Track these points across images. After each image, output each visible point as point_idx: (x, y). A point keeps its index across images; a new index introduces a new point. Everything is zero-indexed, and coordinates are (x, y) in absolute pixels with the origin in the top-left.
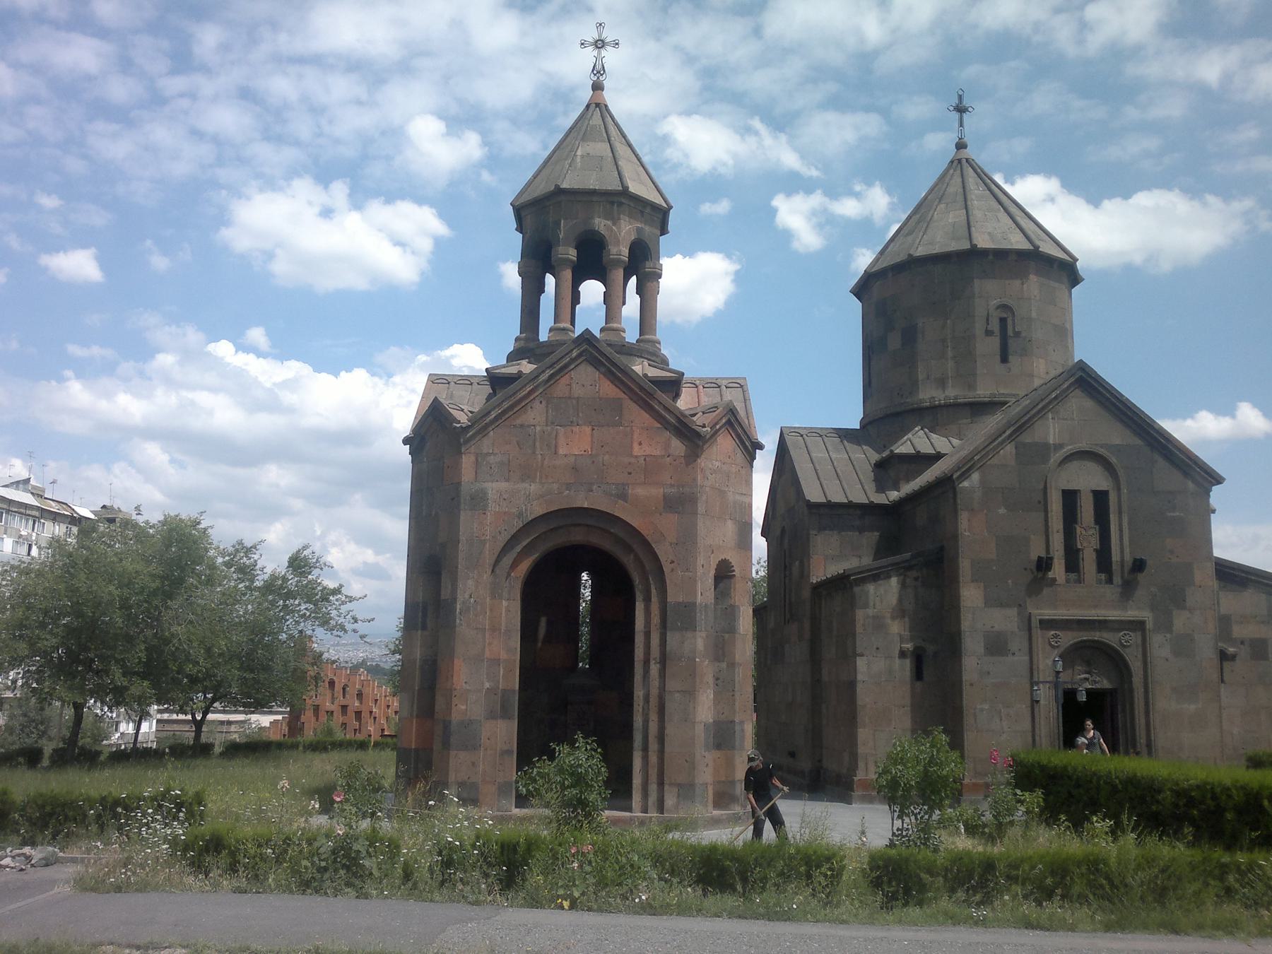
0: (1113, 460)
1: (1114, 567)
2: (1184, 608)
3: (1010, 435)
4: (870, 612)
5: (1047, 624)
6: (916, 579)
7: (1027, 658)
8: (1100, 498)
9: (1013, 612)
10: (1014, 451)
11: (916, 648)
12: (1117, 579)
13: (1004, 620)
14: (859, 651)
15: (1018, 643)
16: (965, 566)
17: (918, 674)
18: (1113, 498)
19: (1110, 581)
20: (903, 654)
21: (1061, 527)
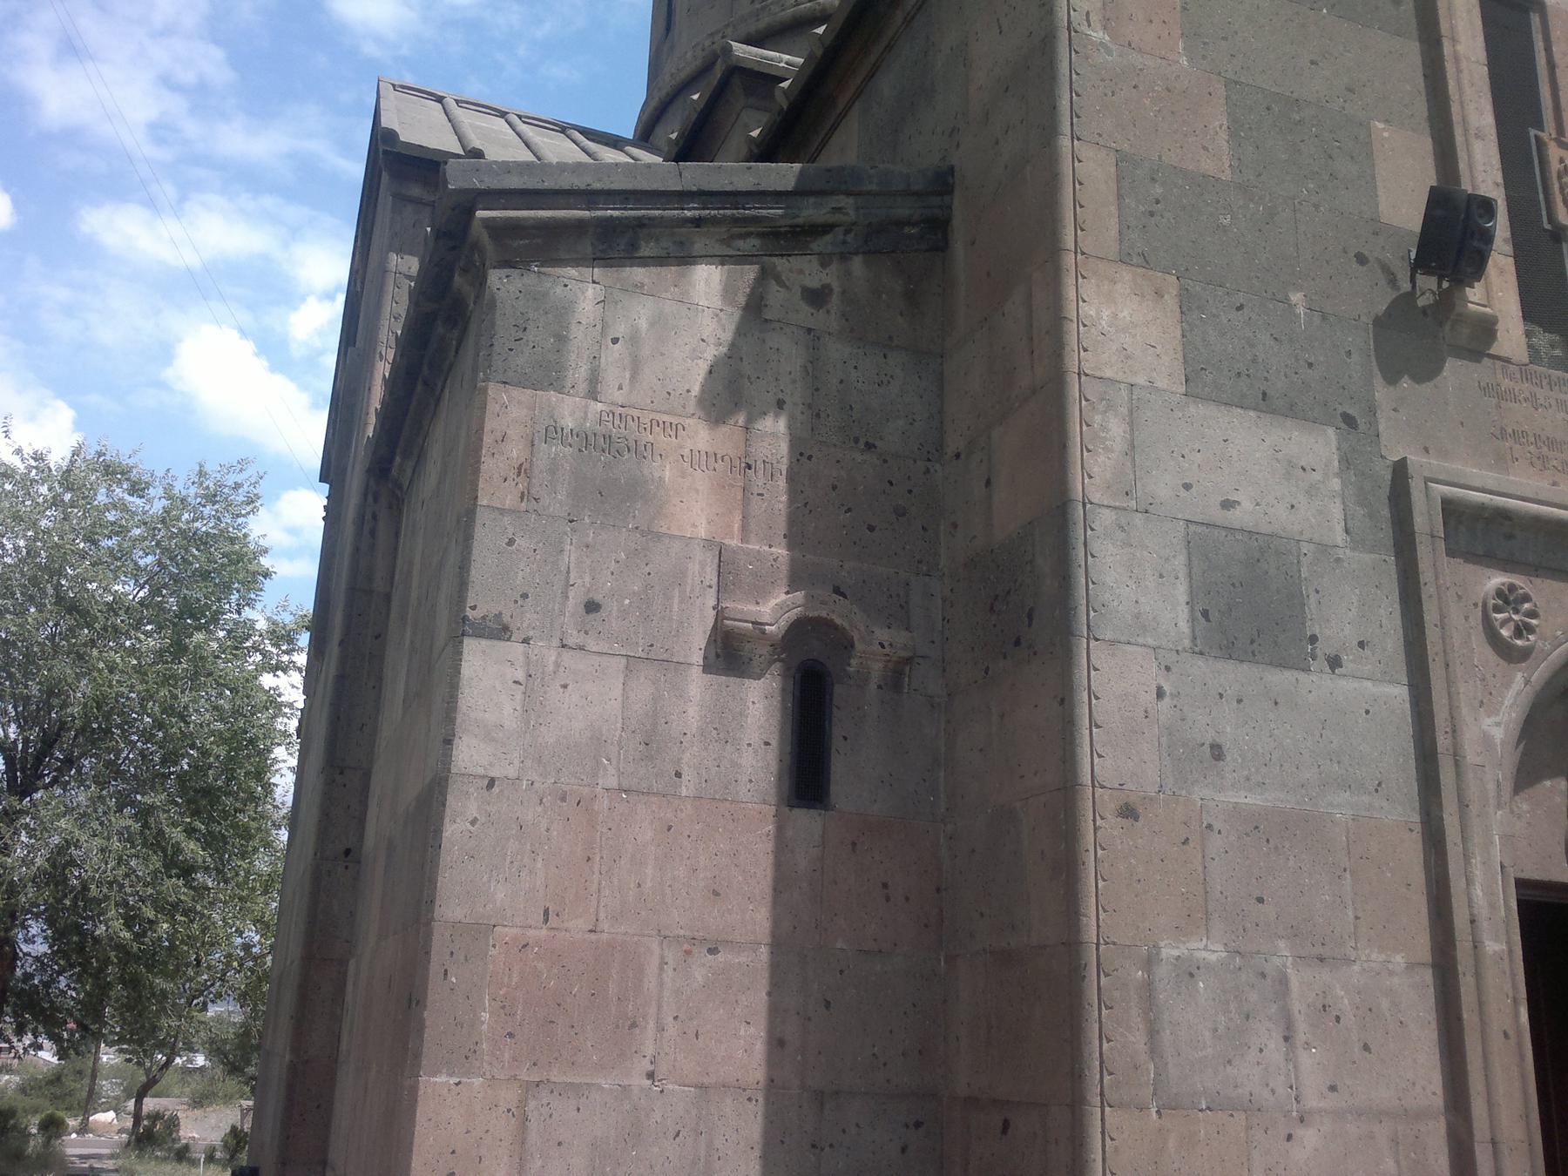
4: (570, 410)
5: (1483, 532)
6: (817, 297)
7: (1398, 694)
9: (1318, 447)
11: (800, 629)
13: (1279, 478)
14: (481, 603)
15: (1352, 607)
16: (1088, 171)
17: (807, 774)
20: (728, 652)
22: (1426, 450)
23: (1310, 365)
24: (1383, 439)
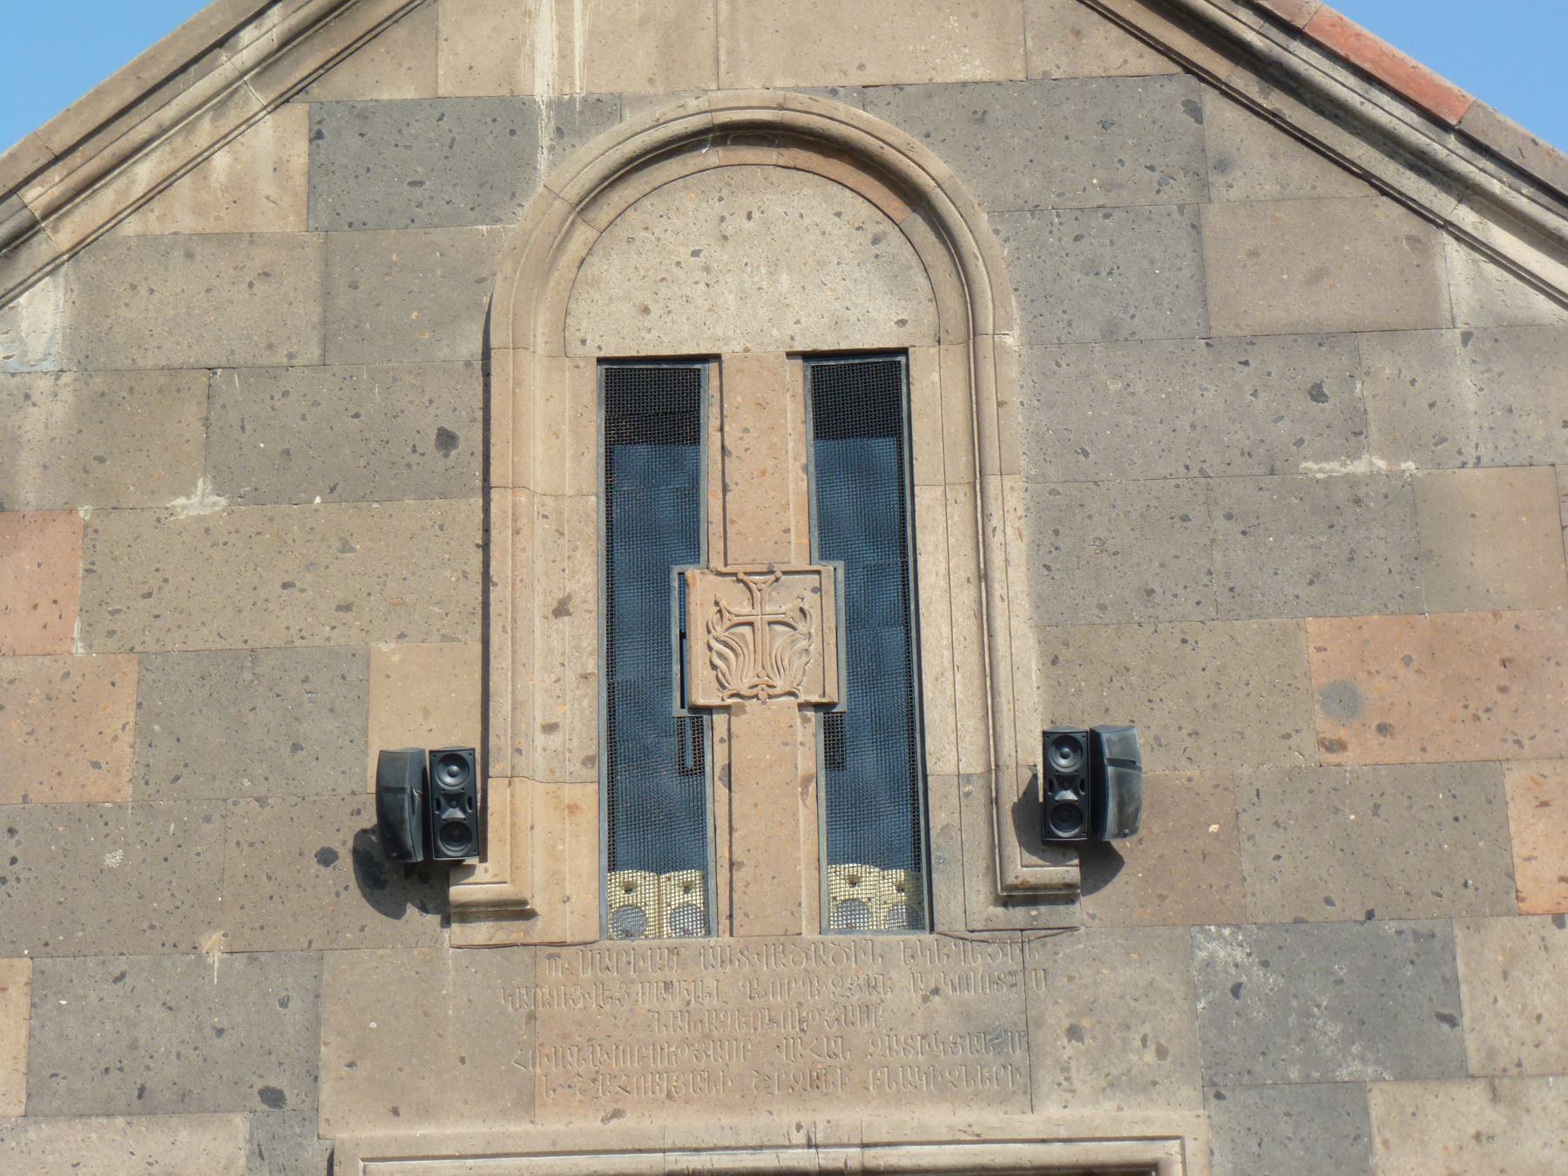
0: (931, 166)
1: (941, 815)
2: (1454, 1070)
3: (267, 64)
8: (857, 398)
10: (299, 154)
12: (963, 894)
18: (932, 394)
19: (919, 915)
21: (585, 579)
22: (395, 1112)
23: (220, 1032)
24: (325, 1113)
